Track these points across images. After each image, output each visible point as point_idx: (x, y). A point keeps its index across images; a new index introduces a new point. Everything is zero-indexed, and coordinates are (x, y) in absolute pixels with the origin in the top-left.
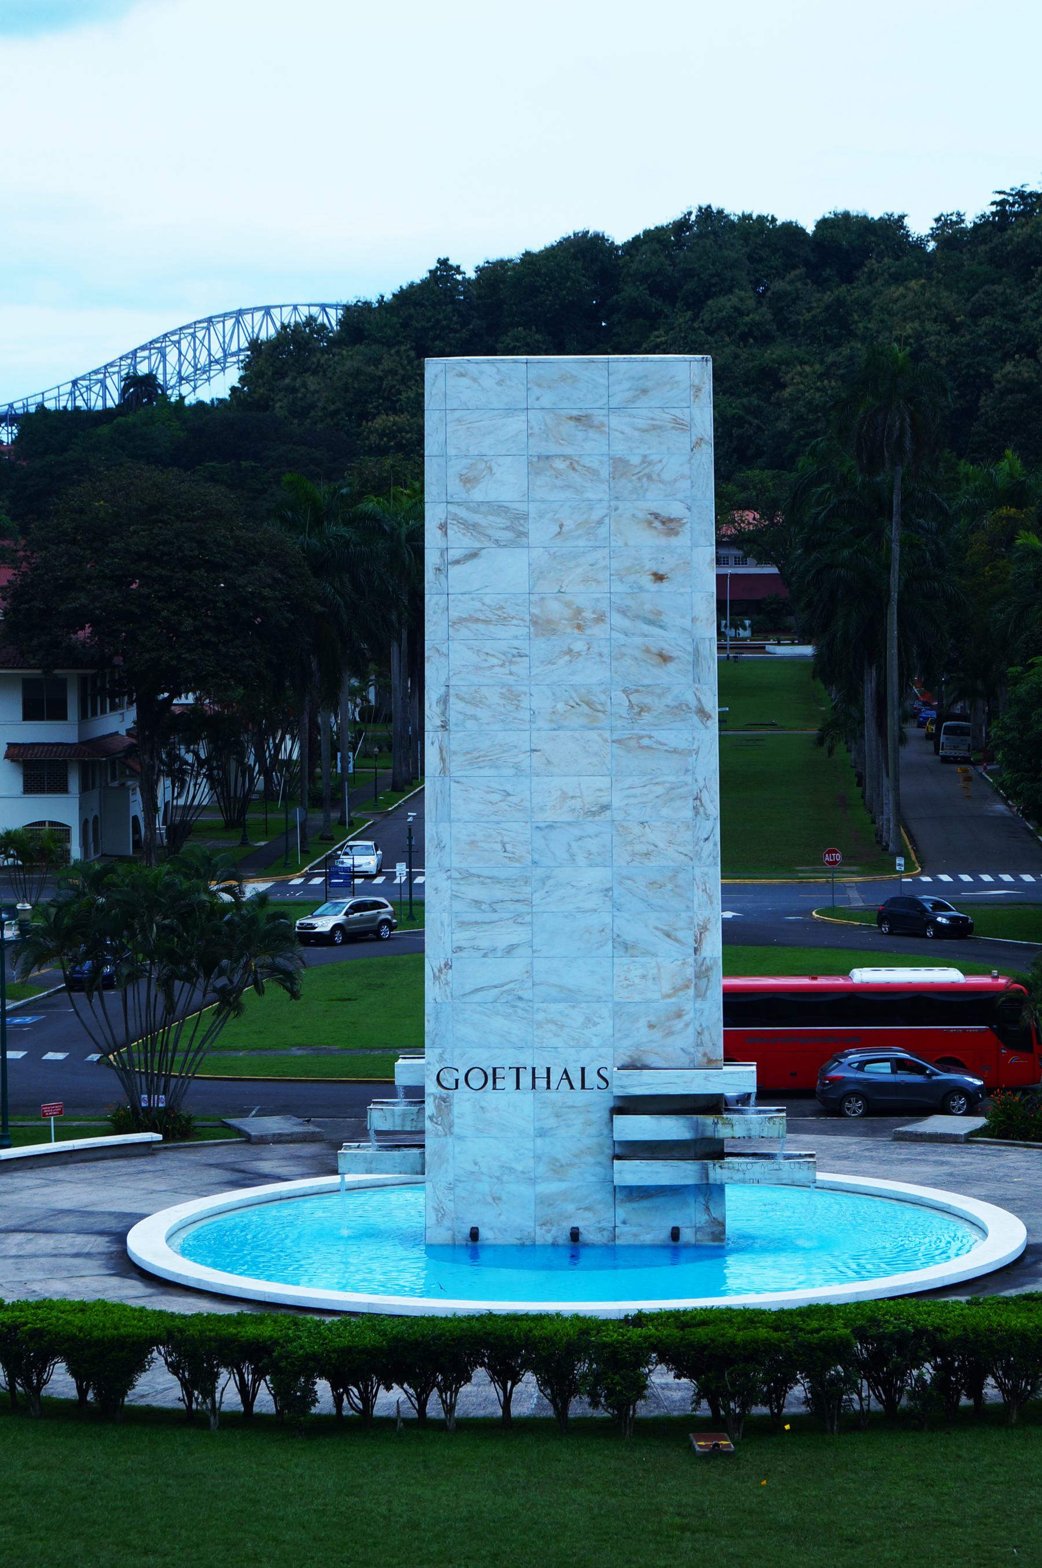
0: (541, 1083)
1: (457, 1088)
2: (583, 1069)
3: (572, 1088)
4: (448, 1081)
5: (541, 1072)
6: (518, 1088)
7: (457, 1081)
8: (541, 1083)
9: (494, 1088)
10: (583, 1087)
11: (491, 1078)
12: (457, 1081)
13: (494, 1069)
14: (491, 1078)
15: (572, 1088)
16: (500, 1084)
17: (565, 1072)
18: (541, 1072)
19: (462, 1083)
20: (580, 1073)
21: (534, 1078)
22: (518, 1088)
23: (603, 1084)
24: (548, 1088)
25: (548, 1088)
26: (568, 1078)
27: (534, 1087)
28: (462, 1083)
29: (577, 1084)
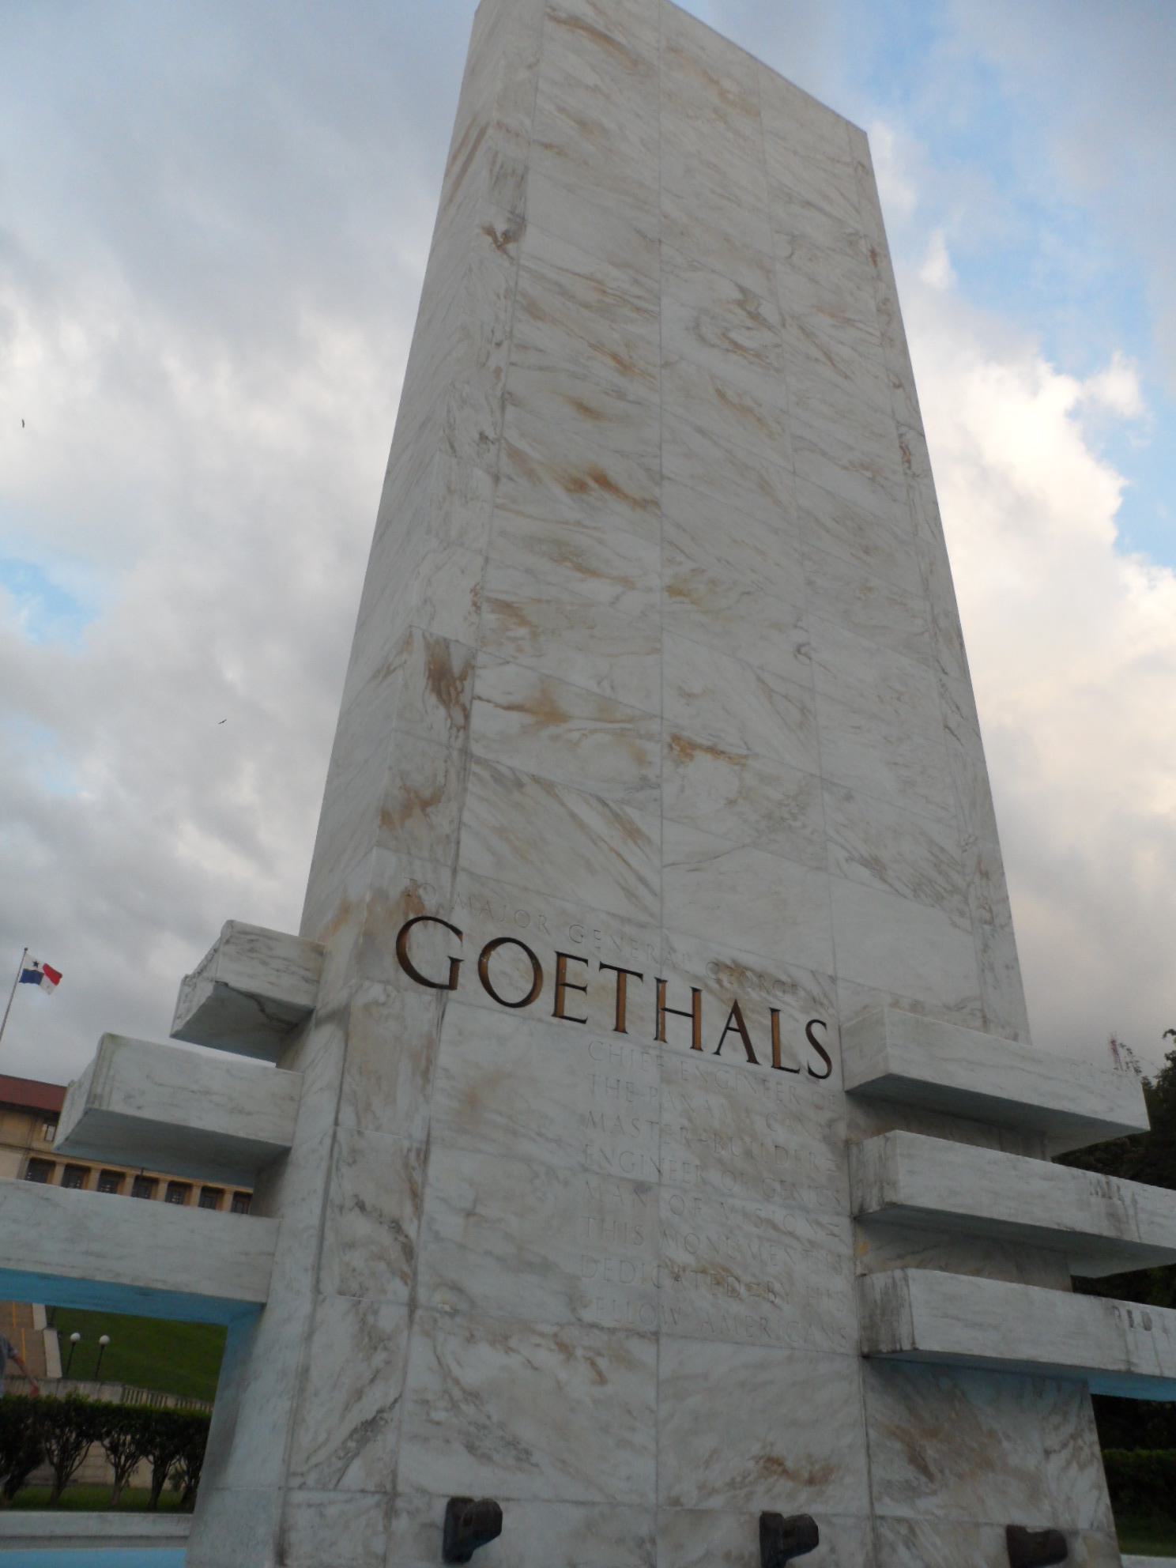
0: (679, 1029)
1: (452, 985)
2: (774, 1012)
3: (752, 1059)
4: (430, 950)
5: (678, 996)
6: (620, 1028)
7: (455, 963)
8: (679, 1029)
9: (558, 1013)
10: (777, 1065)
11: (555, 982)
12: (455, 963)
13: (560, 955)
14: (555, 982)
15: (752, 1059)
16: (573, 1002)
17: (736, 1011)
18: (678, 996)
19: (468, 977)
20: (767, 1021)
21: (662, 1009)
22: (620, 1028)
23: (820, 1067)
24: (696, 1045)
25: (696, 1045)
26: (742, 1030)
27: (660, 1036)
28: (468, 977)
29: (762, 1045)
